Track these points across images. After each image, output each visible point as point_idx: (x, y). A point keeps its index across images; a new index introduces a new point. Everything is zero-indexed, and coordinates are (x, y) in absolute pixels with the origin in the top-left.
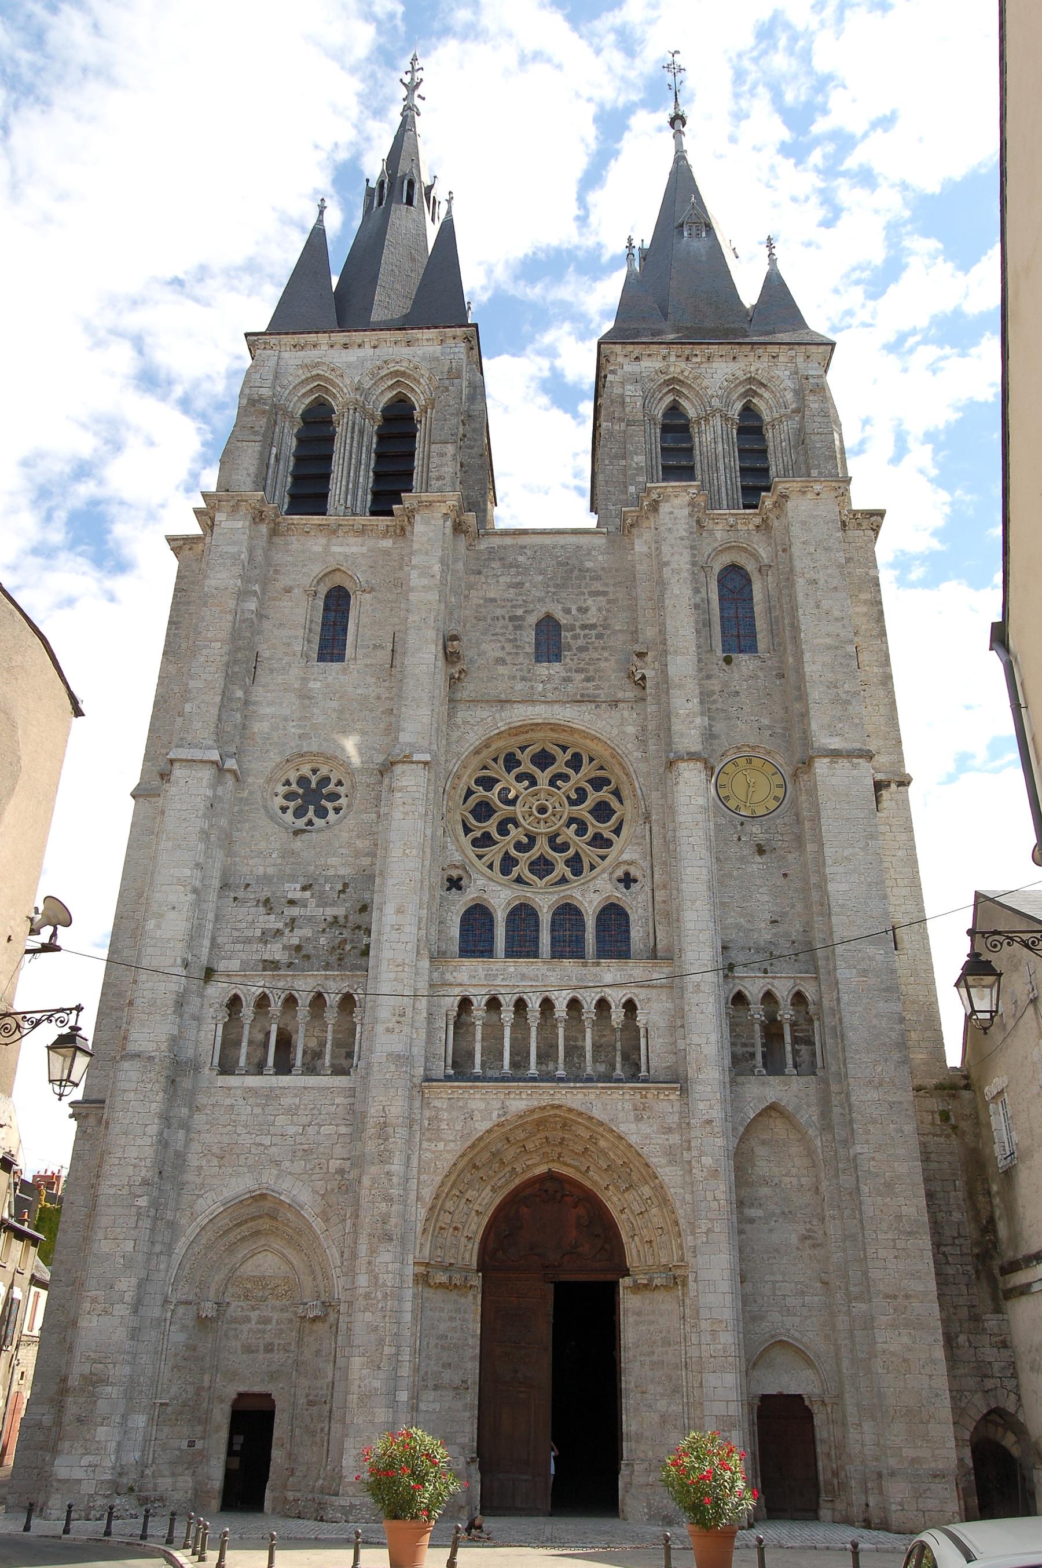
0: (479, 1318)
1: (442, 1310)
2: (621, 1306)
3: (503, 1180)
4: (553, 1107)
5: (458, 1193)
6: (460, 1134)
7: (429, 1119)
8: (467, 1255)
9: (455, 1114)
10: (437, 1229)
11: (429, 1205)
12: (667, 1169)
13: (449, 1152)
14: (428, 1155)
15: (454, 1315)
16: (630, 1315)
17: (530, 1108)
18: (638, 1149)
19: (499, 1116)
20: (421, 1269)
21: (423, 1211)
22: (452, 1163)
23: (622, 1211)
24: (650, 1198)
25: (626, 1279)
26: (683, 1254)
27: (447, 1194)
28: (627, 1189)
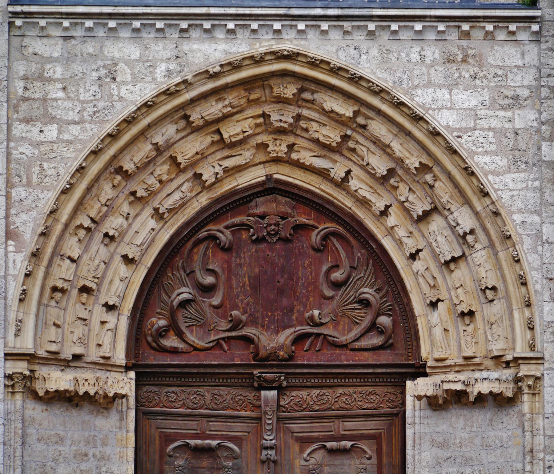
0: (131, 453)
1: (61, 440)
2: (409, 432)
3: (177, 196)
4: (279, 56)
5: (87, 223)
6: (90, 109)
7: (25, 78)
8: (107, 340)
9: (77, 68)
10: (48, 291)
11: (32, 247)
12: (509, 177)
13: (70, 142)
14: (26, 149)
15: (84, 449)
16: (426, 445)
17: (231, 58)
18: (450, 137)
19: (169, 72)
20: (22, 367)
21: (20, 257)
22: (75, 165)
23: (413, 257)
24: (472, 232)
25: (421, 381)
26: (533, 339)
27: (67, 225)
28: (425, 216)
